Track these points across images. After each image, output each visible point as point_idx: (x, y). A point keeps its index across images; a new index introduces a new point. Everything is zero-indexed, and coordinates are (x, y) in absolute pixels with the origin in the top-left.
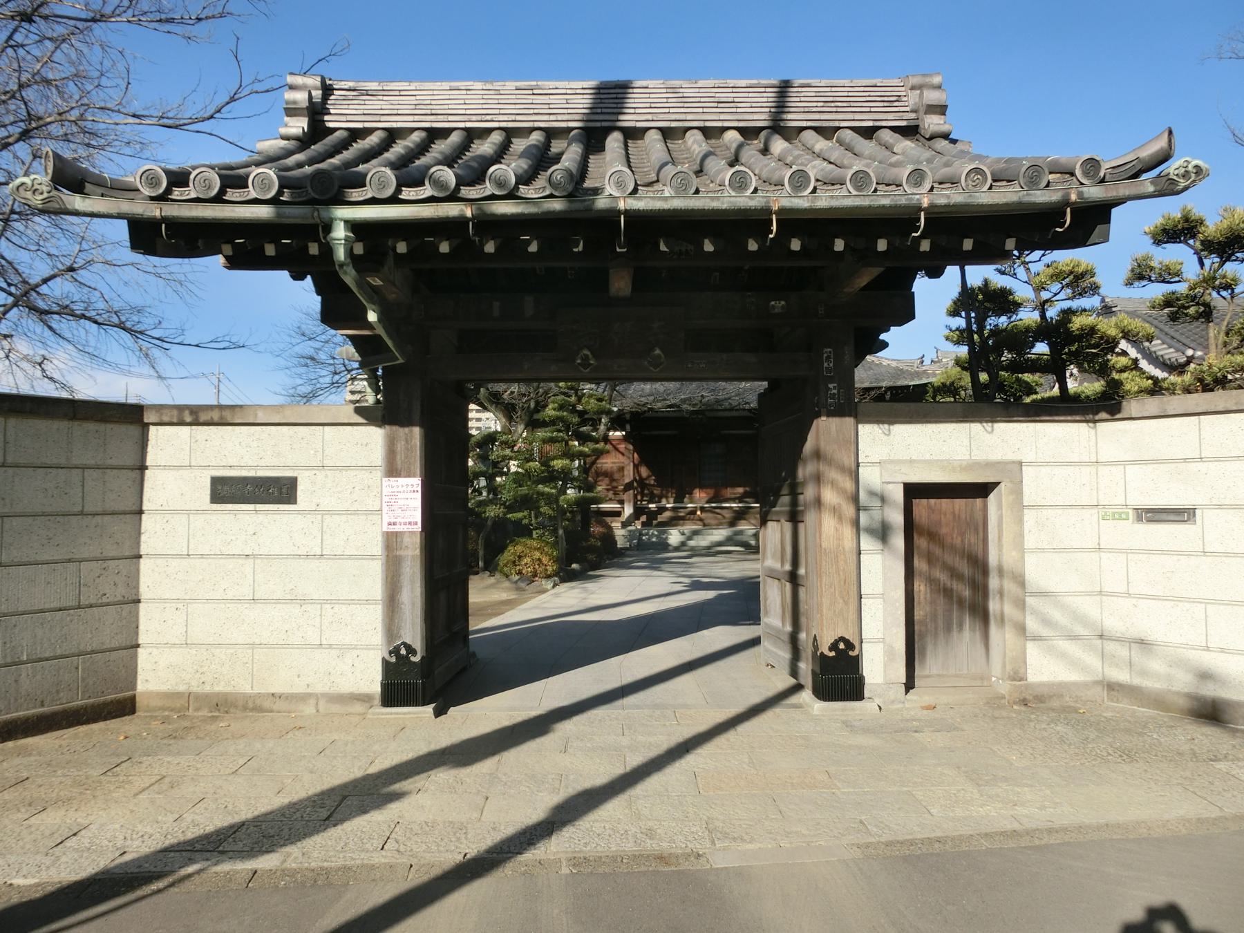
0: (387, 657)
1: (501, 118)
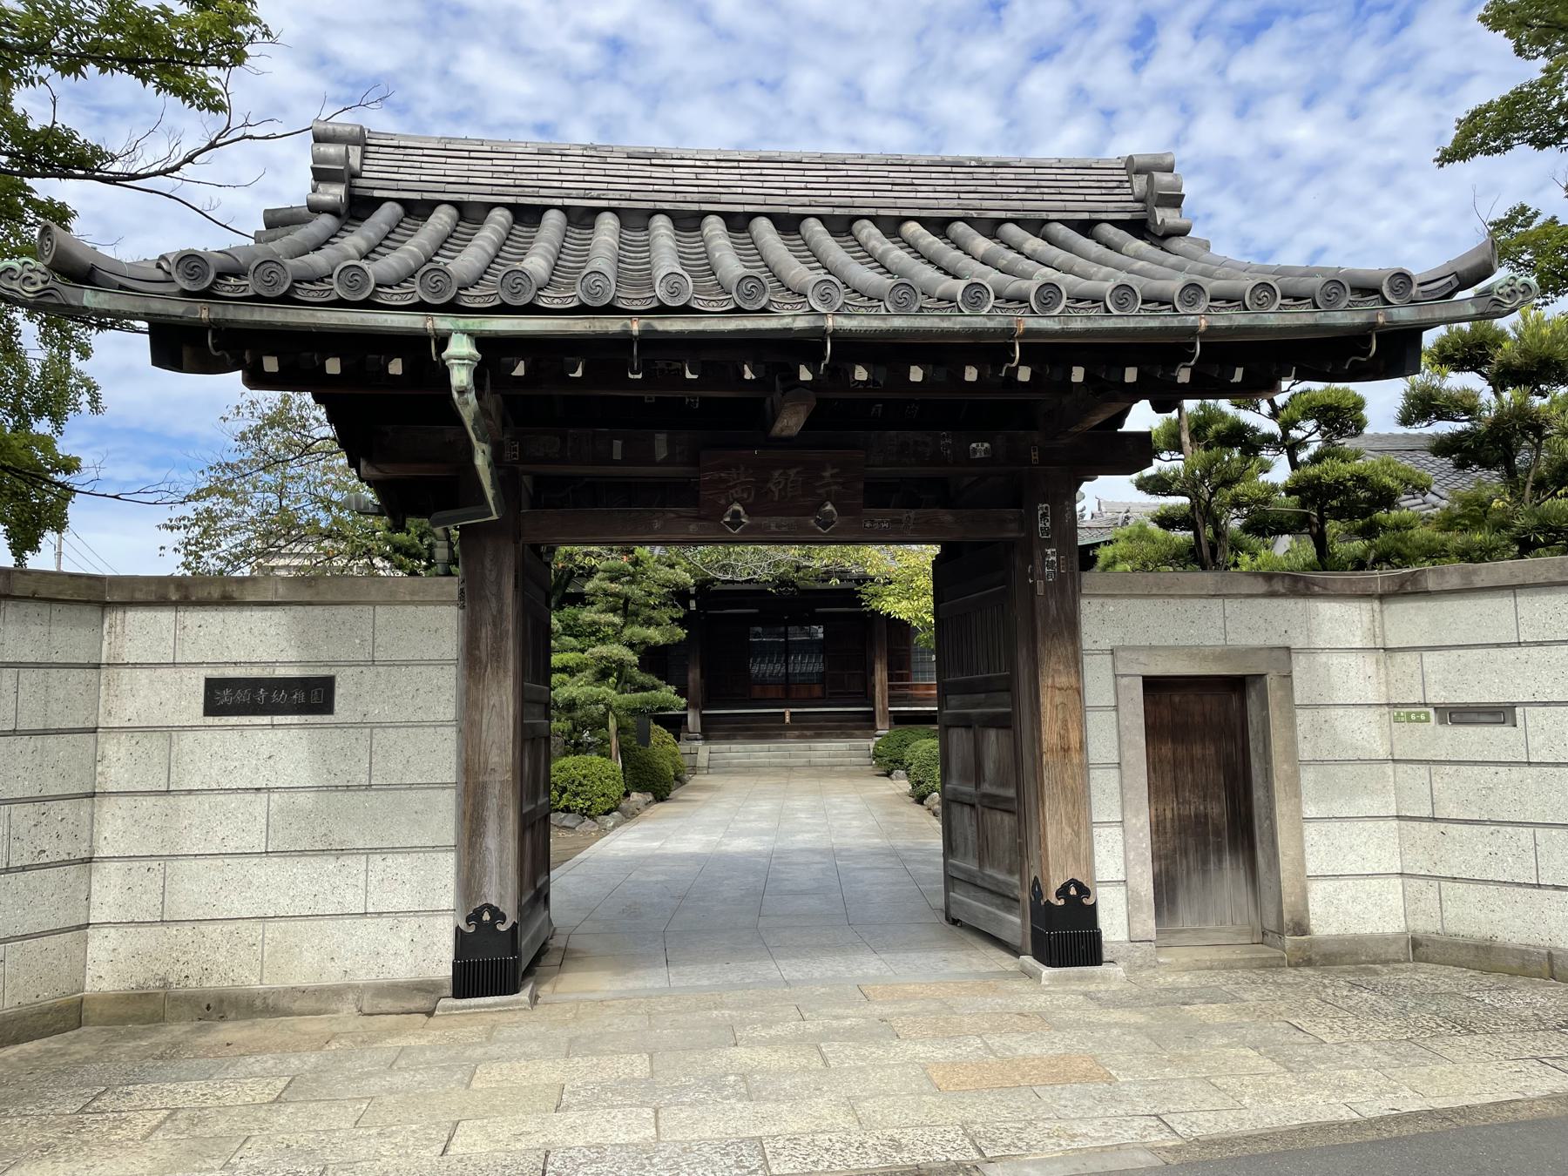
0: (463, 925)
1: (611, 195)
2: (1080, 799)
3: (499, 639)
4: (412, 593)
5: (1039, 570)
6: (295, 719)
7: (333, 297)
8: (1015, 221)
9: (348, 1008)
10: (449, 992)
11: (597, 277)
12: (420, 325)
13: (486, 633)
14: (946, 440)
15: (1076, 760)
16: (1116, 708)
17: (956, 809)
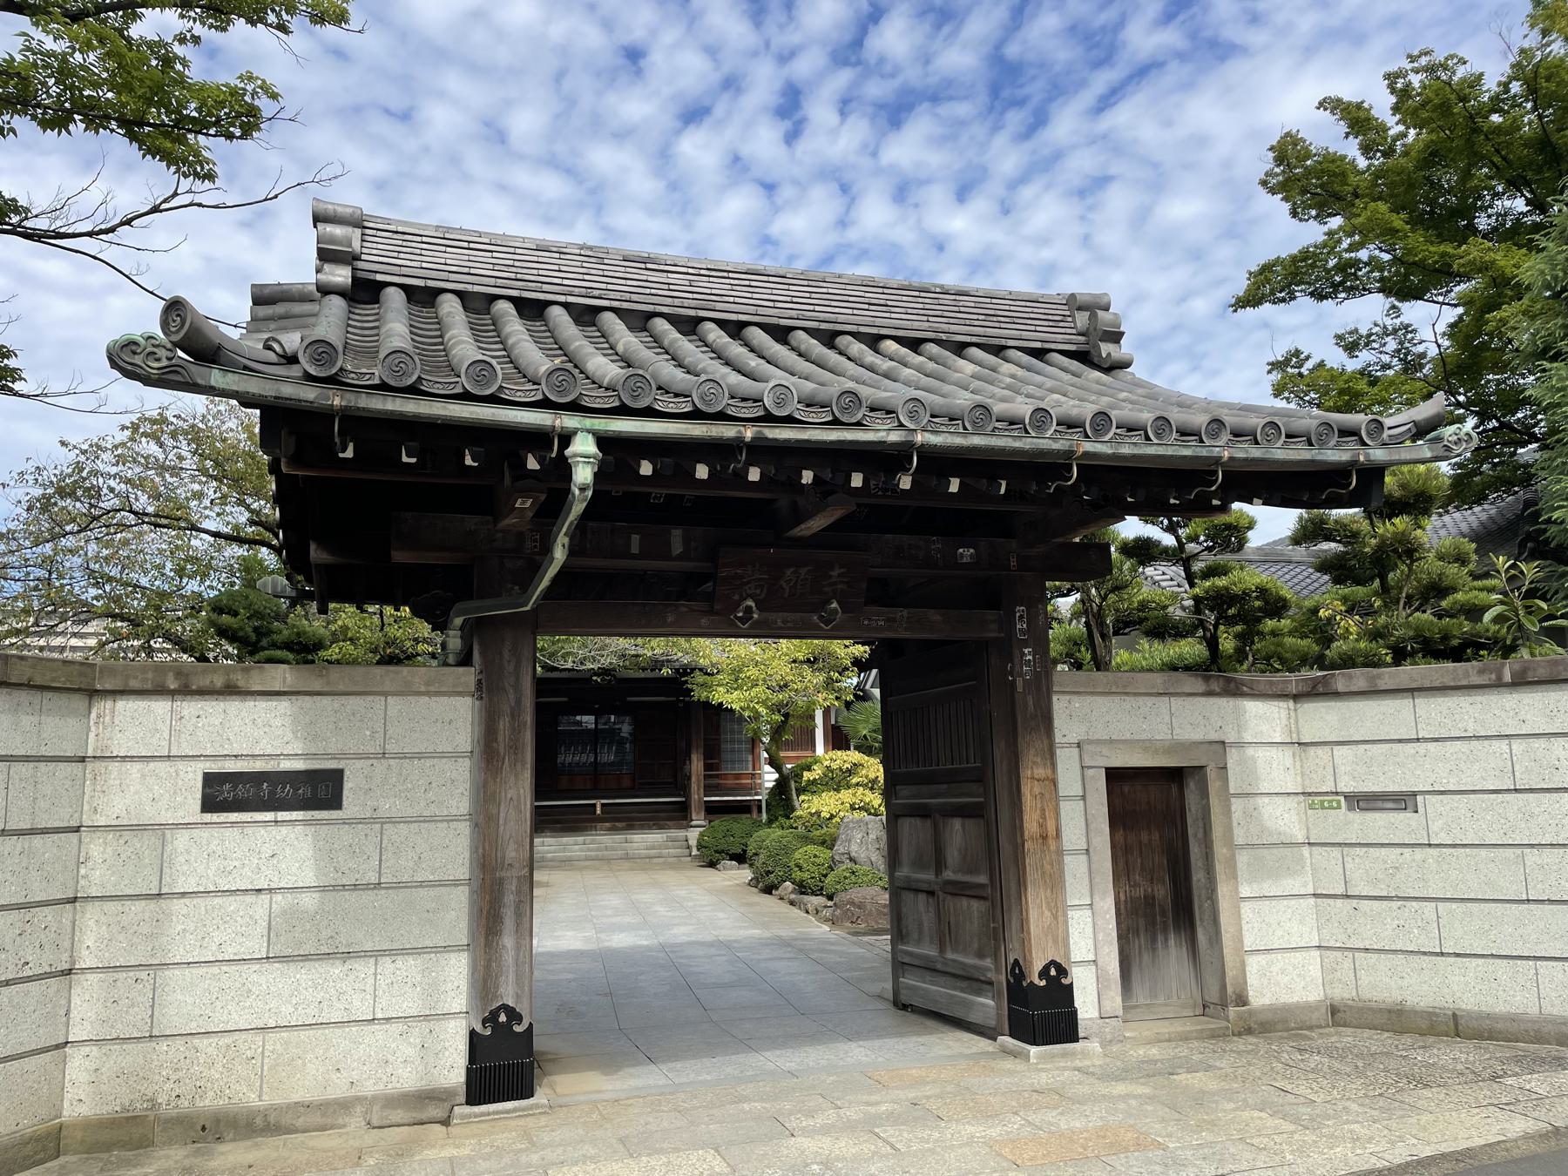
0: (478, 1028)
1: (612, 295)
2: (1056, 882)
3: (516, 730)
4: (427, 684)
5: (1017, 668)
6: (295, 815)
7: (459, 390)
8: (977, 345)
9: (355, 1122)
10: (463, 1099)
11: (712, 384)
12: (549, 423)
13: (504, 725)
14: (936, 544)
15: (1053, 848)
16: (1084, 798)
17: (908, 897)
